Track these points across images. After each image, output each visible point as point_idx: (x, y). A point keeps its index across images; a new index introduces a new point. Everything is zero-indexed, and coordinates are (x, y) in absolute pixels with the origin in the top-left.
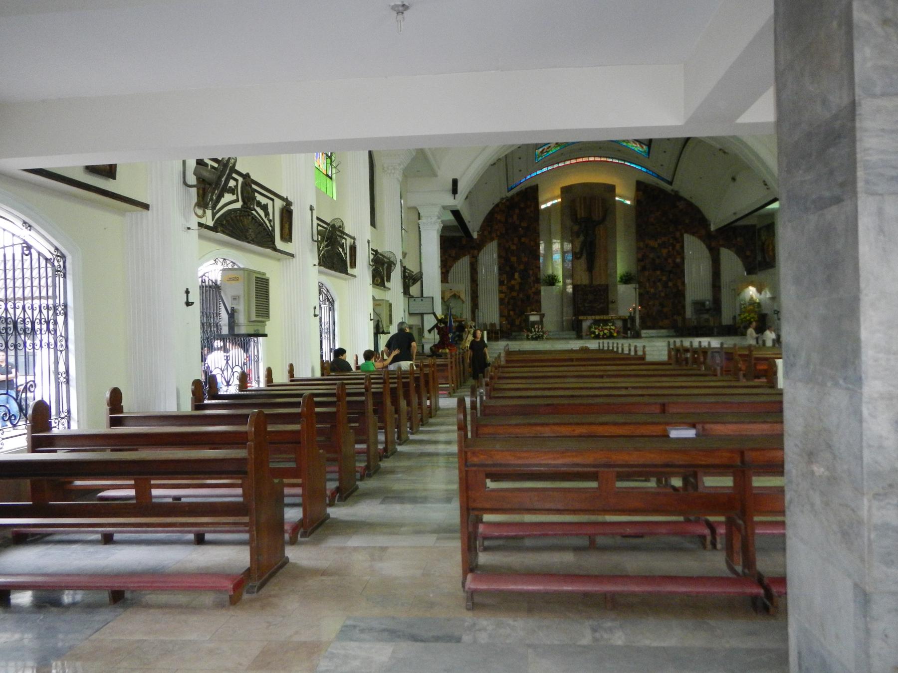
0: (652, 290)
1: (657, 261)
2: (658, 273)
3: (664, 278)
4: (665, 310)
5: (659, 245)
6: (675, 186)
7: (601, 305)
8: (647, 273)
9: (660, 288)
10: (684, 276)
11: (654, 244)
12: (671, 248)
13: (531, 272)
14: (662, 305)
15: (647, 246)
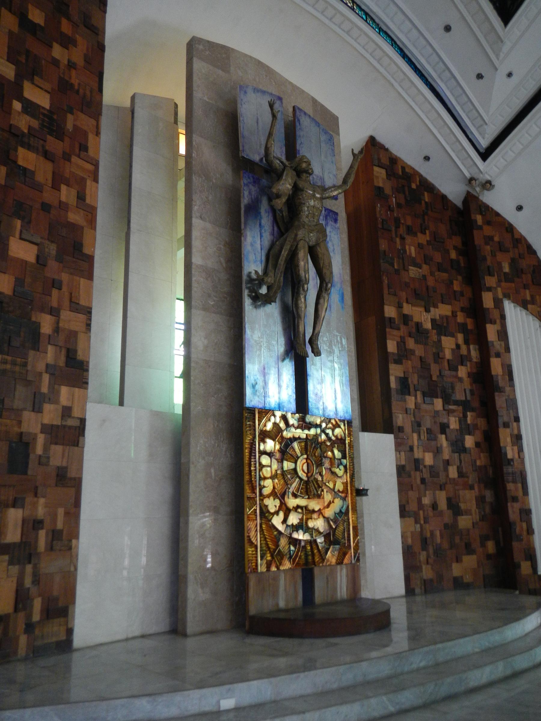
0: (429, 459)
1: (435, 370)
2: (438, 403)
3: (454, 424)
4: (464, 522)
5: (433, 321)
6: (488, 169)
7: (338, 504)
8: (411, 402)
9: (446, 454)
10: (517, 419)
11: (424, 318)
12: (460, 337)
13: (46, 323)
14: (454, 506)
15: (406, 319)
